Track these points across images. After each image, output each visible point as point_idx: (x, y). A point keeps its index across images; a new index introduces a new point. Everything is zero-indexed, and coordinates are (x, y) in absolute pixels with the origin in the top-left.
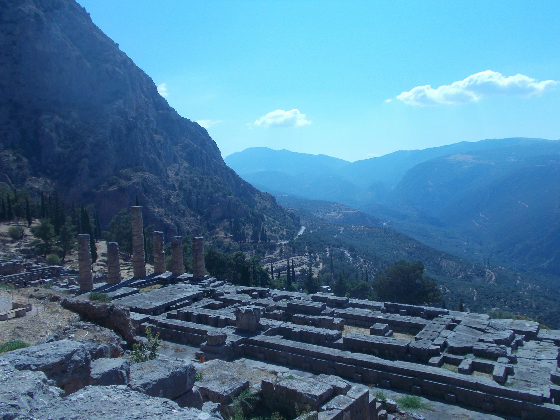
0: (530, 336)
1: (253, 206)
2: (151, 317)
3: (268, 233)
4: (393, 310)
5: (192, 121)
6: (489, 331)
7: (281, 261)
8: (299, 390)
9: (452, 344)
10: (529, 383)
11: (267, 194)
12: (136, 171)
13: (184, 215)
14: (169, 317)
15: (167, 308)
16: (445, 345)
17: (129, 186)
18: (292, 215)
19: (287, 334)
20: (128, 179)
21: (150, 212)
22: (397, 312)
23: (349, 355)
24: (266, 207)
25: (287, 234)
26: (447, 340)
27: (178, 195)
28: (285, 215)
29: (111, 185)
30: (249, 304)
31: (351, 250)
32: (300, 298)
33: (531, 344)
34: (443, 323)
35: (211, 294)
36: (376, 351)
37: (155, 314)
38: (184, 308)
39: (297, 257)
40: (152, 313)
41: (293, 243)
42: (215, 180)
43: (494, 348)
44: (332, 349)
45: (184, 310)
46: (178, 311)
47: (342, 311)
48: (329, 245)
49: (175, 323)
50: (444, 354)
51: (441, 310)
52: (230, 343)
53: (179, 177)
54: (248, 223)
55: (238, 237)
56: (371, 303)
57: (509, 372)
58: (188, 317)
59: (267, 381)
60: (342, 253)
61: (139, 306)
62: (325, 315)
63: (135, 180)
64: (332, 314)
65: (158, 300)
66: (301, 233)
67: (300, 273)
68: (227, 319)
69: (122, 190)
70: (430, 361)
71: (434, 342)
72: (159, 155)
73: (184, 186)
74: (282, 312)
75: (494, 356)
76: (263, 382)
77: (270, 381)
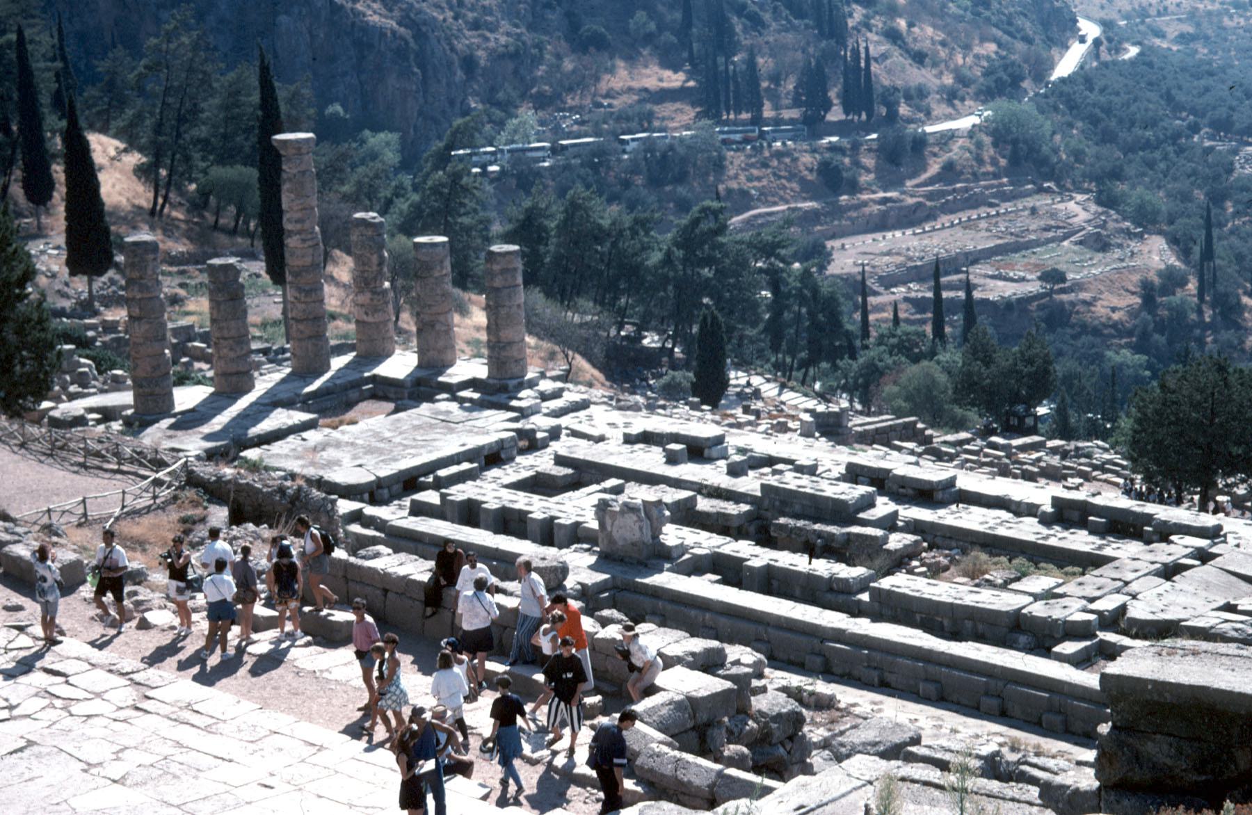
2: (370, 510)
14: (419, 510)
15: (409, 482)
23: (863, 626)
37: (374, 501)
38: (460, 487)
39: (1030, 202)
40: (366, 496)
45: (460, 492)
46: (443, 496)
52: (579, 587)
58: (470, 513)
62: (864, 523)
64: (890, 523)
68: (577, 525)
70: (1057, 649)
74: (745, 508)
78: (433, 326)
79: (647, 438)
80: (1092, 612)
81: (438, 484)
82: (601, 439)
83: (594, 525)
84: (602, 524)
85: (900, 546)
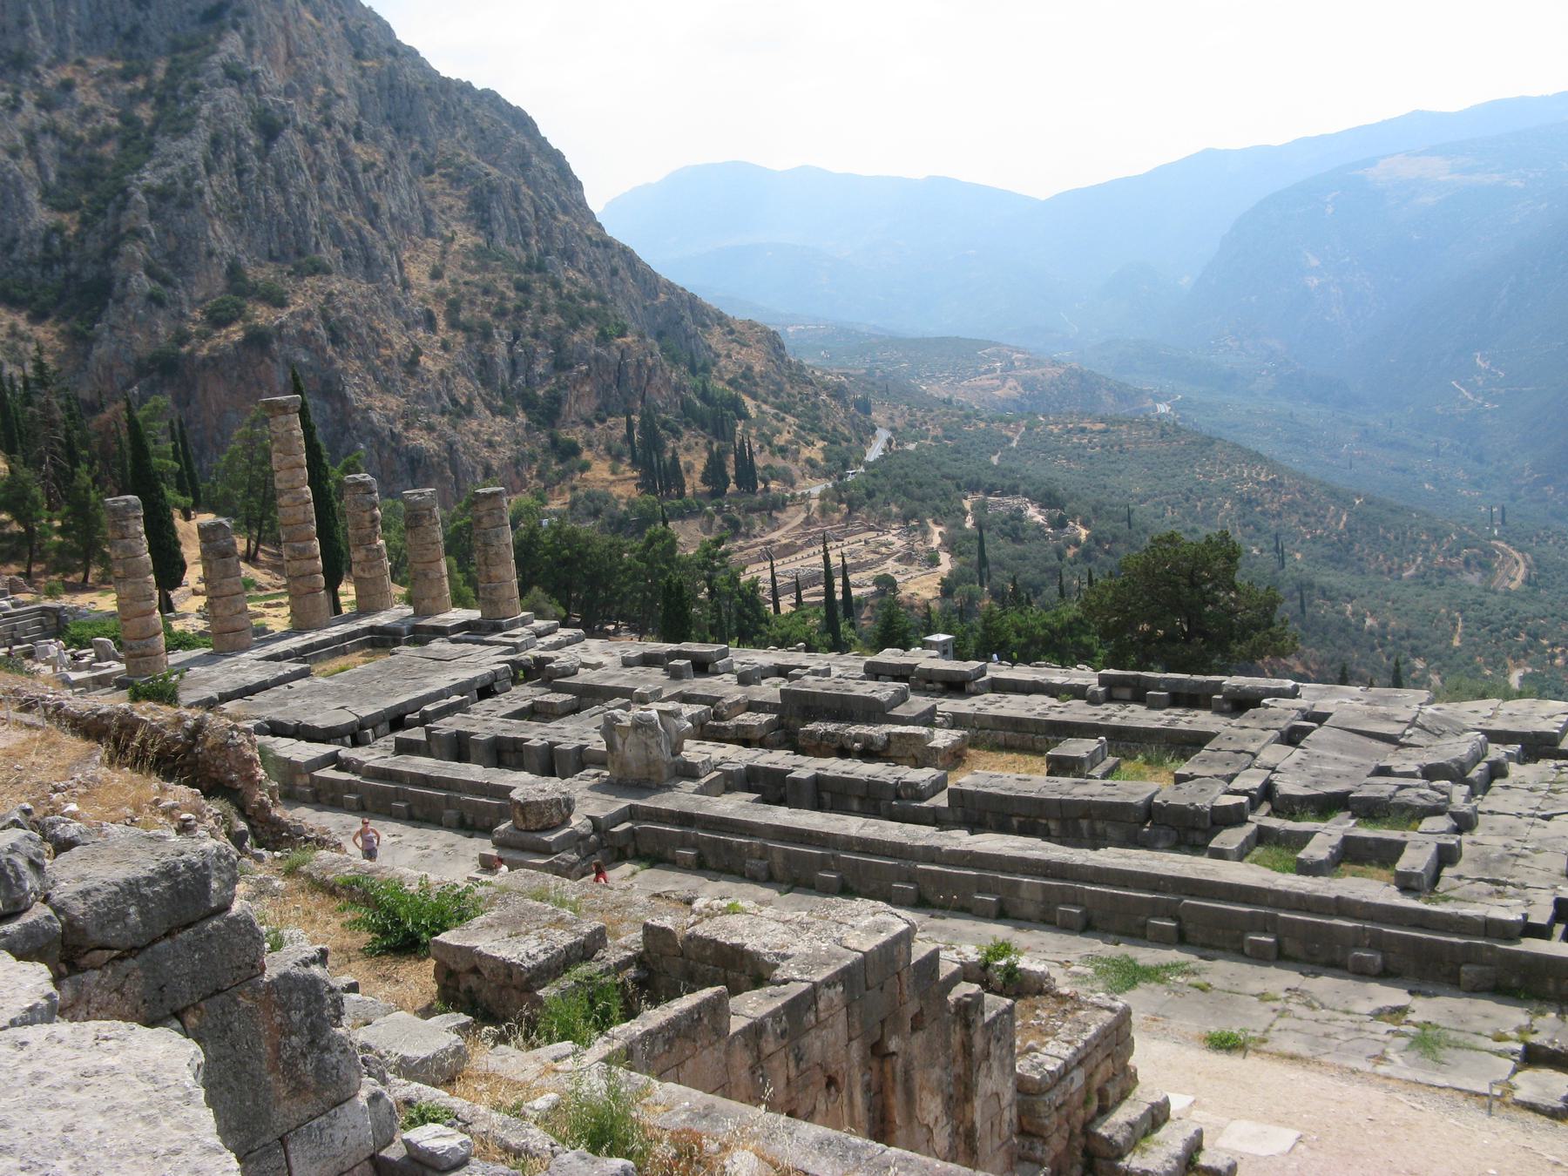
1: (705, 369)
2: (345, 752)
3: (760, 461)
4: (1126, 693)
5: (479, 86)
6: (1412, 741)
7: (811, 551)
8: (751, 944)
9: (1288, 785)
10: (1501, 888)
11: (751, 325)
12: (299, 273)
13: (468, 411)
14: (404, 748)
15: (396, 720)
16: (1268, 791)
17: (282, 326)
18: (838, 393)
19: (772, 787)
20: (277, 300)
21: (356, 409)
22: (1139, 698)
23: (960, 840)
24: (750, 368)
25: (827, 459)
26: (1273, 777)
27: (445, 346)
28: (817, 394)
29: (218, 320)
30: (662, 698)
31: (1048, 500)
32: (827, 673)
34: (1271, 724)
35: (537, 671)
36: (1052, 825)
37: (356, 743)
38: (448, 720)
39: (863, 536)
40: (348, 739)
41: (846, 488)
42: (567, 288)
43: (1419, 792)
44: (909, 827)
45: (449, 725)
46: (428, 731)
47: (964, 706)
48: (973, 487)
49: (417, 766)
50: (1262, 818)
51: (1275, 683)
52: (589, 822)
53: (444, 284)
54: (688, 426)
55: (660, 476)
56: (1058, 676)
57: (1447, 856)
58: (460, 747)
59: (657, 923)
60: (1018, 515)
61: (308, 719)
63: (299, 302)
64: (928, 718)
65: (363, 698)
66: (874, 453)
67: (874, 588)
69: (258, 340)
71: (1237, 784)
72: (372, 212)
73: (464, 316)
74: (765, 718)
75: (1413, 814)
76: (646, 926)
77: (667, 922)
78: (426, 575)
79: (648, 660)
80: (1236, 793)
81: (424, 720)
82: (599, 665)
84: (611, 746)
85: (948, 743)
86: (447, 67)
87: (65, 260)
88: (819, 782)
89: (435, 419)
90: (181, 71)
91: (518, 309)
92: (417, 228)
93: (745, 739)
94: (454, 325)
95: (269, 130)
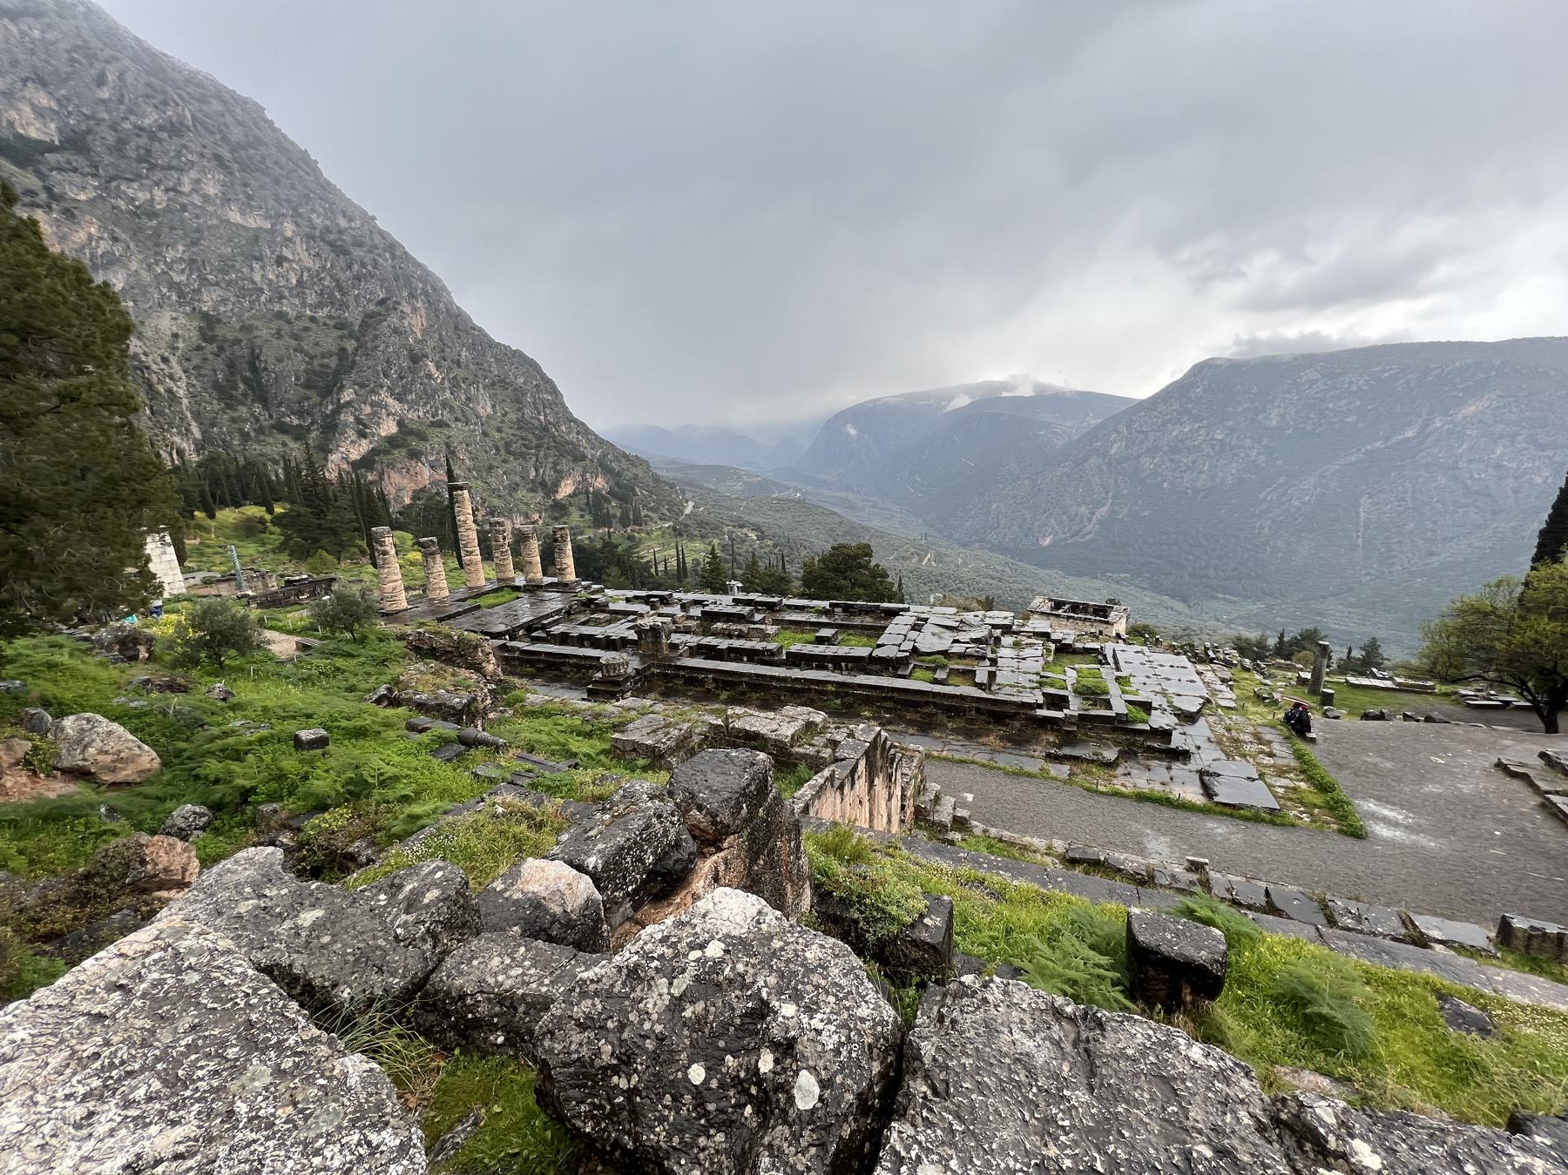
0: (1007, 630)
9: (923, 649)
16: (915, 650)
31: (757, 528)
33: (1008, 640)
43: (973, 649)
45: (557, 629)
57: (992, 675)
58: (564, 639)
66: (688, 511)
83: (635, 637)
86: (497, 336)
87: (311, 415)
88: (731, 649)
89: (504, 493)
90: (369, 326)
91: (538, 447)
92: (489, 410)
93: (687, 631)
94: (509, 452)
95: (415, 359)
